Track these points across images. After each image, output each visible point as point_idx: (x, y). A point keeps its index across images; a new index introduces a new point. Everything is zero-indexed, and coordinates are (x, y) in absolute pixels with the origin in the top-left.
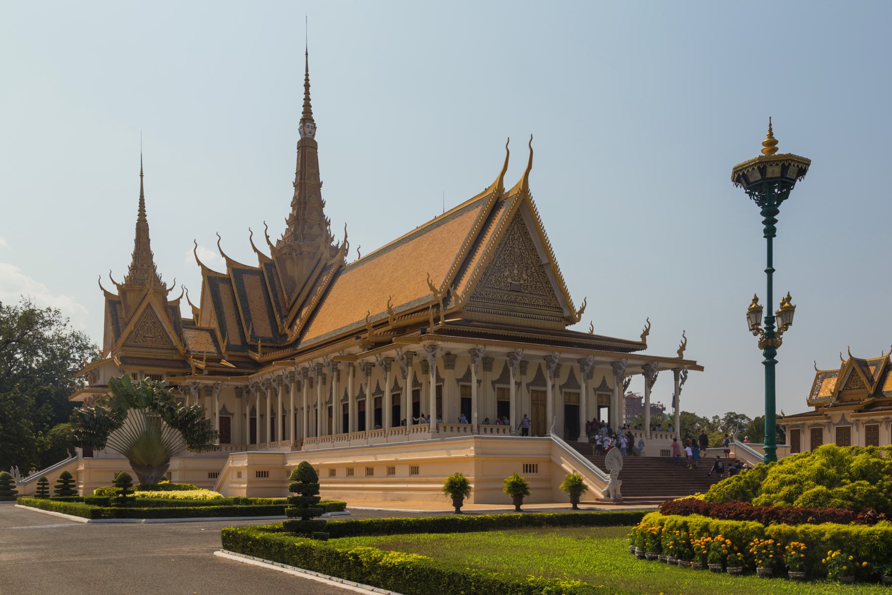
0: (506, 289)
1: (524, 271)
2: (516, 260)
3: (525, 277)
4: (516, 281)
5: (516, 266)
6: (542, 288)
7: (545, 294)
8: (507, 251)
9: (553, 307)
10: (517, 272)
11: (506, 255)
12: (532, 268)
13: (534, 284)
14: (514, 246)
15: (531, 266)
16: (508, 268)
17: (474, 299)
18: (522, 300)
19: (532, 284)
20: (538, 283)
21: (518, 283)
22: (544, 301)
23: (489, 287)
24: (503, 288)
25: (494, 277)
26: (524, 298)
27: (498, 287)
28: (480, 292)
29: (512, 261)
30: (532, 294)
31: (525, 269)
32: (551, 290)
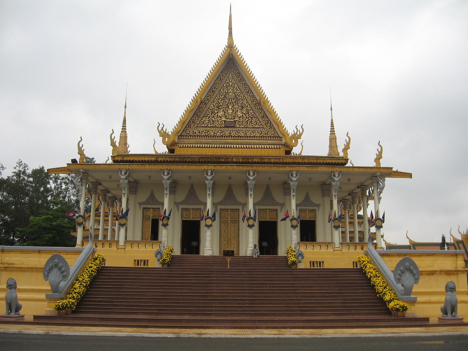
0: (220, 126)
2: (230, 102)
3: (239, 114)
4: (231, 119)
5: (230, 107)
6: (258, 122)
8: (222, 96)
10: (232, 111)
12: (247, 107)
13: (249, 120)
17: (187, 138)
18: (237, 133)
19: (247, 119)
20: (253, 118)
21: (233, 120)
23: (203, 127)
24: (216, 126)
25: (207, 118)
27: (211, 126)
29: (226, 104)
30: (247, 128)
31: (240, 108)
32: (269, 122)
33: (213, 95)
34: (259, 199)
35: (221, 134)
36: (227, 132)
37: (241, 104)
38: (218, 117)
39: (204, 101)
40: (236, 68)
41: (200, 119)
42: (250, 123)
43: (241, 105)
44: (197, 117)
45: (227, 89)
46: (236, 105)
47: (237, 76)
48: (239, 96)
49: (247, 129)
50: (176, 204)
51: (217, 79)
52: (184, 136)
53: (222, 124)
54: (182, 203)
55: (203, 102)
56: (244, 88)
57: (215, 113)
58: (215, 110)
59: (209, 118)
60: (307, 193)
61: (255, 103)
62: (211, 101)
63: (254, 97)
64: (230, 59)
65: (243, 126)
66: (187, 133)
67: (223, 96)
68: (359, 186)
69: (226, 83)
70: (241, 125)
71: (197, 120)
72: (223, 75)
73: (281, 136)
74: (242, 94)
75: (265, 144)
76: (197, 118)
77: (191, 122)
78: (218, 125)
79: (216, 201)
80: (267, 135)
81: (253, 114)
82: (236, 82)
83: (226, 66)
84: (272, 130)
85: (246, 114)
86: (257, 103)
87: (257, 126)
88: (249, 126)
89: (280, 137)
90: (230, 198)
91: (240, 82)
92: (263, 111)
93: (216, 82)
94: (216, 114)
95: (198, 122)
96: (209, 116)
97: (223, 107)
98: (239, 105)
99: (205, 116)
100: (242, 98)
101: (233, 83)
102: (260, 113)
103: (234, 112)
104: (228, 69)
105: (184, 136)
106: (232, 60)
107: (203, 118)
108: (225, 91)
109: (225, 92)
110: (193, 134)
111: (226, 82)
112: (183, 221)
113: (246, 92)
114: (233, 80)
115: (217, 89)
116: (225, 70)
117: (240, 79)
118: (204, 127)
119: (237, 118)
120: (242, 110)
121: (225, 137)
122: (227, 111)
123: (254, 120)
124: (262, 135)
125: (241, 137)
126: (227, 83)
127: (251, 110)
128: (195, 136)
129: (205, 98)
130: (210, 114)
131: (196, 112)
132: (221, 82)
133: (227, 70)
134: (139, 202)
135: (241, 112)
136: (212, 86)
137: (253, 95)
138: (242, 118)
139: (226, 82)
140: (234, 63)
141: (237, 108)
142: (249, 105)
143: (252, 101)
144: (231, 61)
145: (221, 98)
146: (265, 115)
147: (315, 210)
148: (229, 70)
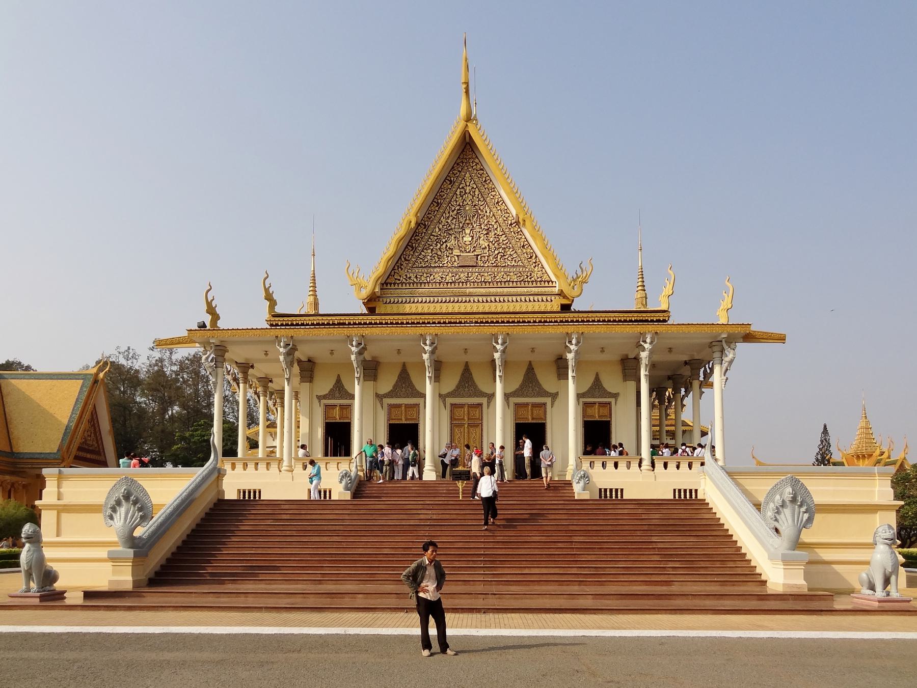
0: (450, 265)
1: (482, 235)
3: (484, 244)
4: (469, 252)
5: (468, 231)
7: (521, 264)
8: (453, 211)
9: (536, 281)
10: (470, 239)
11: (451, 218)
14: (465, 203)
15: (495, 227)
16: (453, 236)
18: (479, 277)
19: (496, 252)
20: (507, 250)
21: (473, 254)
22: (519, 274)
23: (422, 267)
24: (445, 265)
26: (482, 274)
28: (406, 275)
29: (461, 225)
30: (496, 266)
33: (437, 211)
34: (515, 385)
35: (454, 279)
36: (462, 275)
37: (486, 225)
38: (447, 249)
39: (423, 222)
40: (477, 161)
41: (417, 254)
42: (501, 258)
43: (486, 228)
44: (412, 250)
45: (462, 198)
46: (477, 227)
47: (479, 176)
48: (482, 211)
49: (496, 269)
50: (379, 397)
51: (445, 181)
52: (391, 284)
53: (455, 261)
54: (389, 395)
55: (422, 224)
56: (492, 197)
57: (442, 243)
58: (442, 238)
59: (432, 252)
60: (597, 375)
61: (510, 223)
62: (435, 221)
63: (508, 211)
64: (467, 143)
65: (489, 265)
66: (396, 279)
67: (455, 212)
68: (688, 362)
69: (460, 189)
70: (486, 262)
71: (412, 255)
72: (455, 175)
73: (553, 279)
74: (487, 207)
75: (527, 294)
76: (412, 252)
77: (403, 259)
78: (447, 263)
79: (445, 391)
80: (530, 278)
81: (507, 243)
82: (477, 187)
83: (459, 157)
84: (540, 269)
85: (494, 242)
86: (514, 223)
87: (513, 263)
88: (499, 264)
89: (552, 282)
90: (467, 385)
91: (484, 186)
92: (523, 237)
93: (442, 187)
94: (444, 246)
95: (413, 259)
96: (432, 247)
97: (456, 232)
98: (483, 226)
99: (426, 249)
100: (488, 214)
101: (473, 188)
102: (518, 240)
103: (474, 240)
104: (463, 163)
105: (391, 284)
106: (470, 146)
107: (423, 251)
108: (458, 203)
109: (459, 205)
110: (407, 280)
111: (461, 187)
112: (390, 425)
113: (494, 204)
114: (473, 182)
115: (445, 199)
116: (458, 164)
117: (484, 179)
118: (424, 267)
119: (480, 251)
120: (487, 237)
121: (459, 285)
122: (463, 239)
123: (508, 253)
124: (522, 279)
125: (486, 282)
126: (463, 188)
127: (503, 234)
128: (410, 283)
129: (426, 216)
130: (433, 245)
131: (409, 242)
132: (452, 186)
133: (462, 165)
134: (317, 395)
135: (486, 239)
136: (436, 195)
137: (506, 208)
138: (488, 249)
139: (461, 187)
140: (472, 150)
141: (479, 232)
142: (500, 226)
143: (505, 219)
144: (468, 147)
145: (451, 216)
146: (526, 243)
147: (610, 403)
148: (464, 164)
